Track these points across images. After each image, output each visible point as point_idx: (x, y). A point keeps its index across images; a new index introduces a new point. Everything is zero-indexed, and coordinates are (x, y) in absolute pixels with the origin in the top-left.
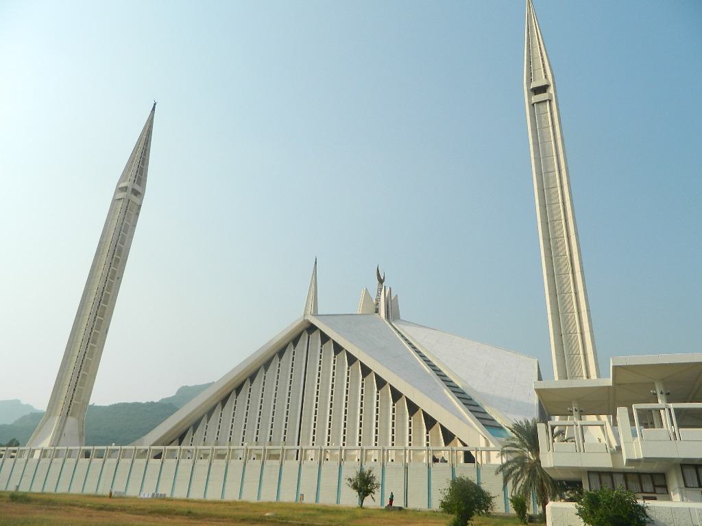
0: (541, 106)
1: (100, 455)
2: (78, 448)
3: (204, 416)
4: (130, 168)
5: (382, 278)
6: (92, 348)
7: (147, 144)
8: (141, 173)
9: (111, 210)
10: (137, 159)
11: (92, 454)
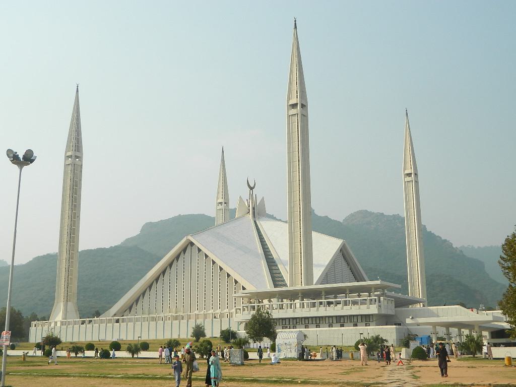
0: (293, 118)
1: (90, 321)
2: (78, 320)
3: (140, 296)
4: (71, 140)
5: (252, 186)
6: (72, 262)
7: (78, 119)
8: (78, 143)
9: (65, 172)
10: (74, 135)
11: (87, 322)
